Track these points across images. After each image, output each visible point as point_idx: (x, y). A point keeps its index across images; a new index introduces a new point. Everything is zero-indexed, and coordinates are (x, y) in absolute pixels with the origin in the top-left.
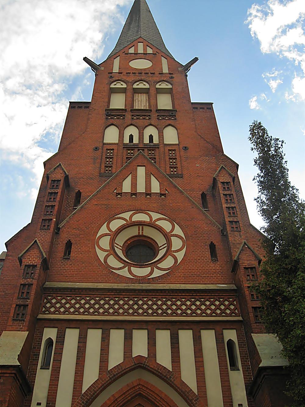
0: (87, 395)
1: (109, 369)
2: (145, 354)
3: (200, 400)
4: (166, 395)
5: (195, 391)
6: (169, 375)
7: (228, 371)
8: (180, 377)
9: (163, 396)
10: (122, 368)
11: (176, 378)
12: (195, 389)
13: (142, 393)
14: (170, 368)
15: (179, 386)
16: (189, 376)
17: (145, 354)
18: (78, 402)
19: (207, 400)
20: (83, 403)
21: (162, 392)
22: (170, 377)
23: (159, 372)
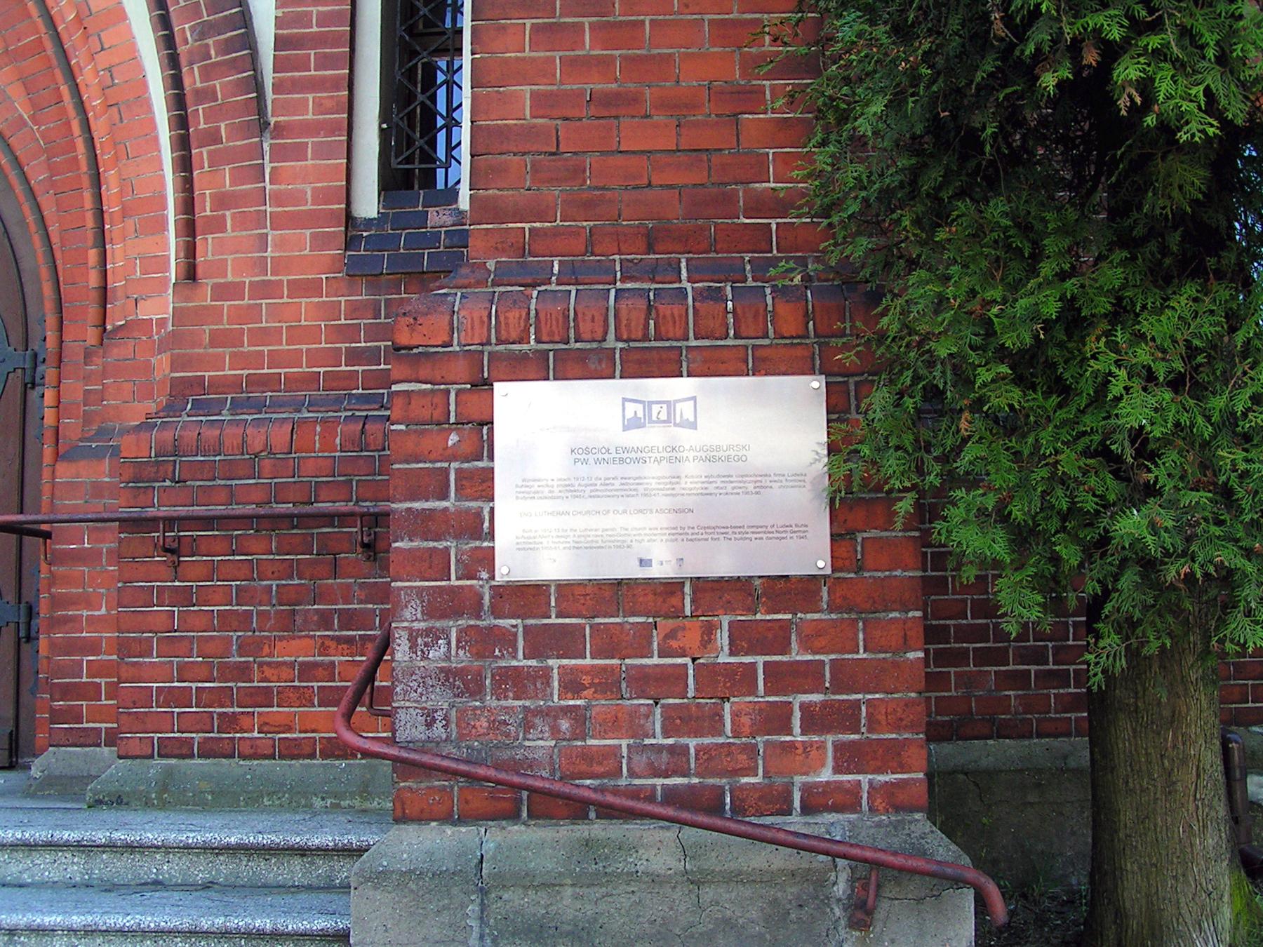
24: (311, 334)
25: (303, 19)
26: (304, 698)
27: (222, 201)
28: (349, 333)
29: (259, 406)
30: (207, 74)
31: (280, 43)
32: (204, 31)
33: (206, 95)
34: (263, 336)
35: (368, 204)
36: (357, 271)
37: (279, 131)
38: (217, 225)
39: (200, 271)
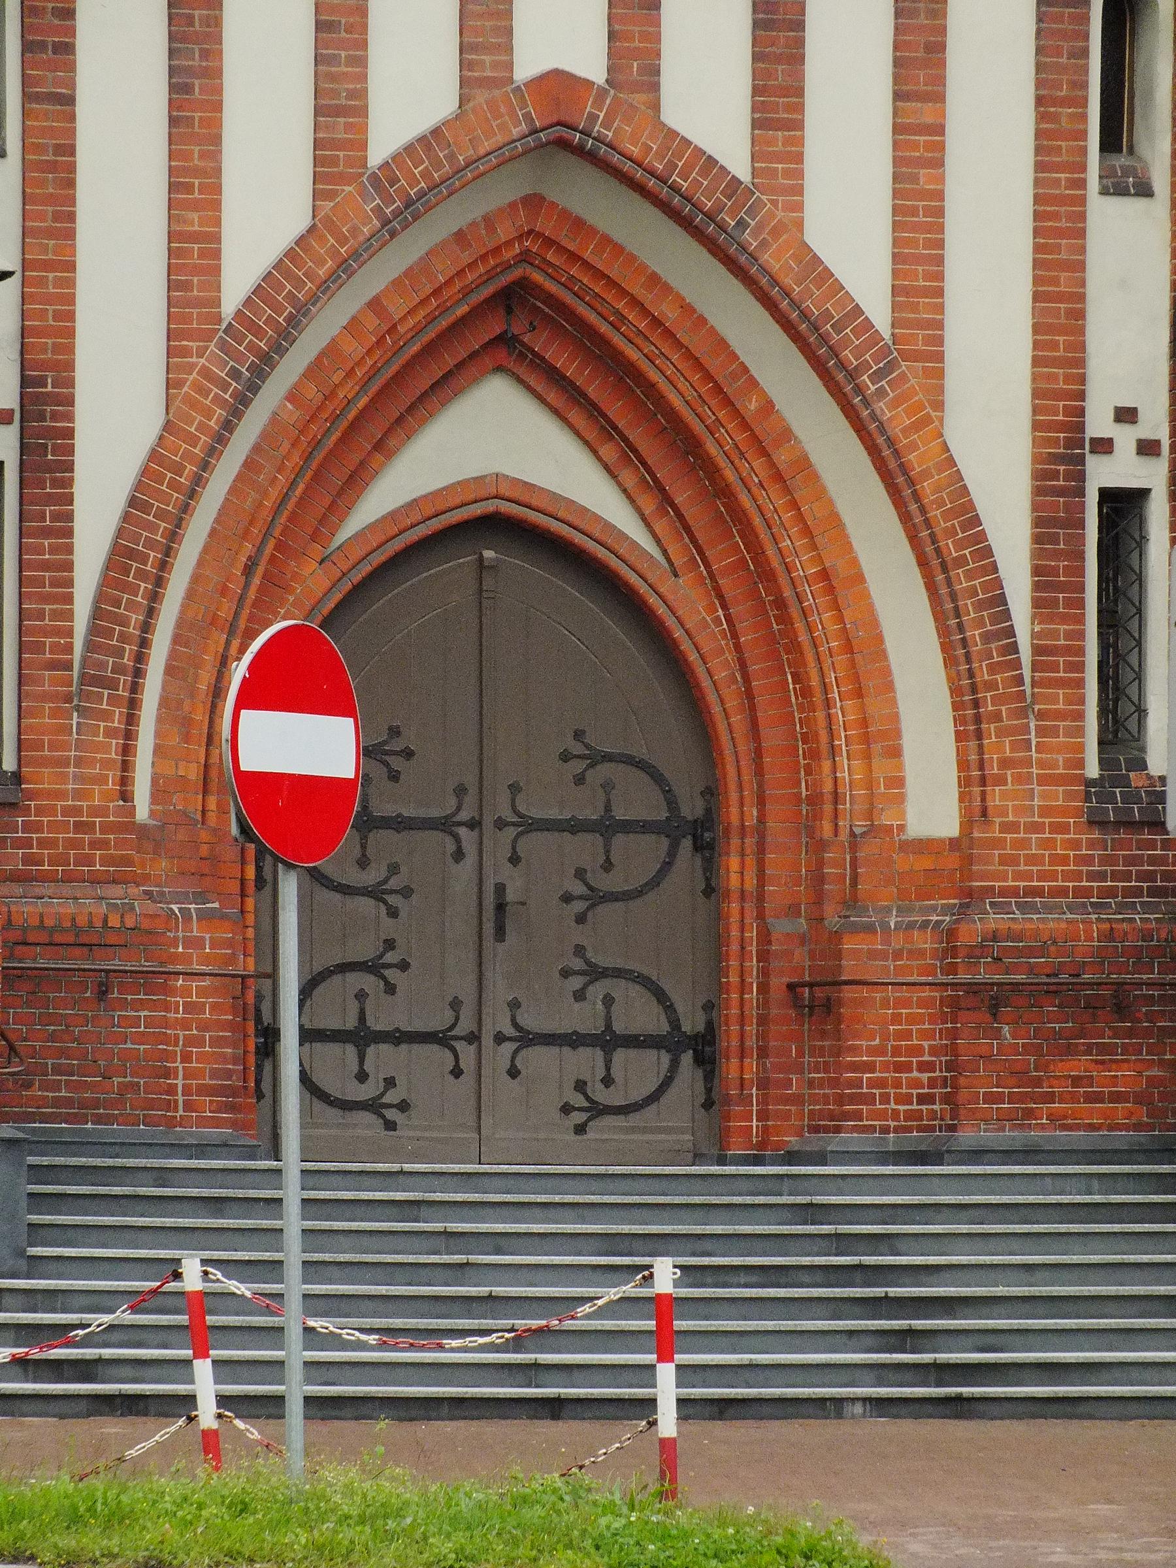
0: (258, 332)
1: (379, 151)
2: (590, 62)
3: (903, 377)
4: (687, 309)
5: (878, 310)
6: (733, 213)
7: (1082, 201)
8: (799, 224)
9: (669, 313)
10: (451, 157)
11: (776, 232)
12: (878, 310)
13: (538, 277)
14: (739, 165)
15: (788, 281)
16: (846, 229)
17: (590, 62)
18: (205, 373)
19: (940, 374)
20: (235, 374)
21: (667, 289)
22: (742, 224)
23: (675, 188)
24: (1064, 860)
25: (1054, 635)
26: (1074, 1098)
27: (1005, 763)
28: (1088, 860)
29: (1033, 909)
30: (992, 669)
31: (1037, 650)
32: (987, 638)
33: (991, 686)
34: (1032, 860)
35: (1093, 770)
36: (1096, 822)
37: (1041, 716)
38: (1001, 781)
39: (990, 812)
